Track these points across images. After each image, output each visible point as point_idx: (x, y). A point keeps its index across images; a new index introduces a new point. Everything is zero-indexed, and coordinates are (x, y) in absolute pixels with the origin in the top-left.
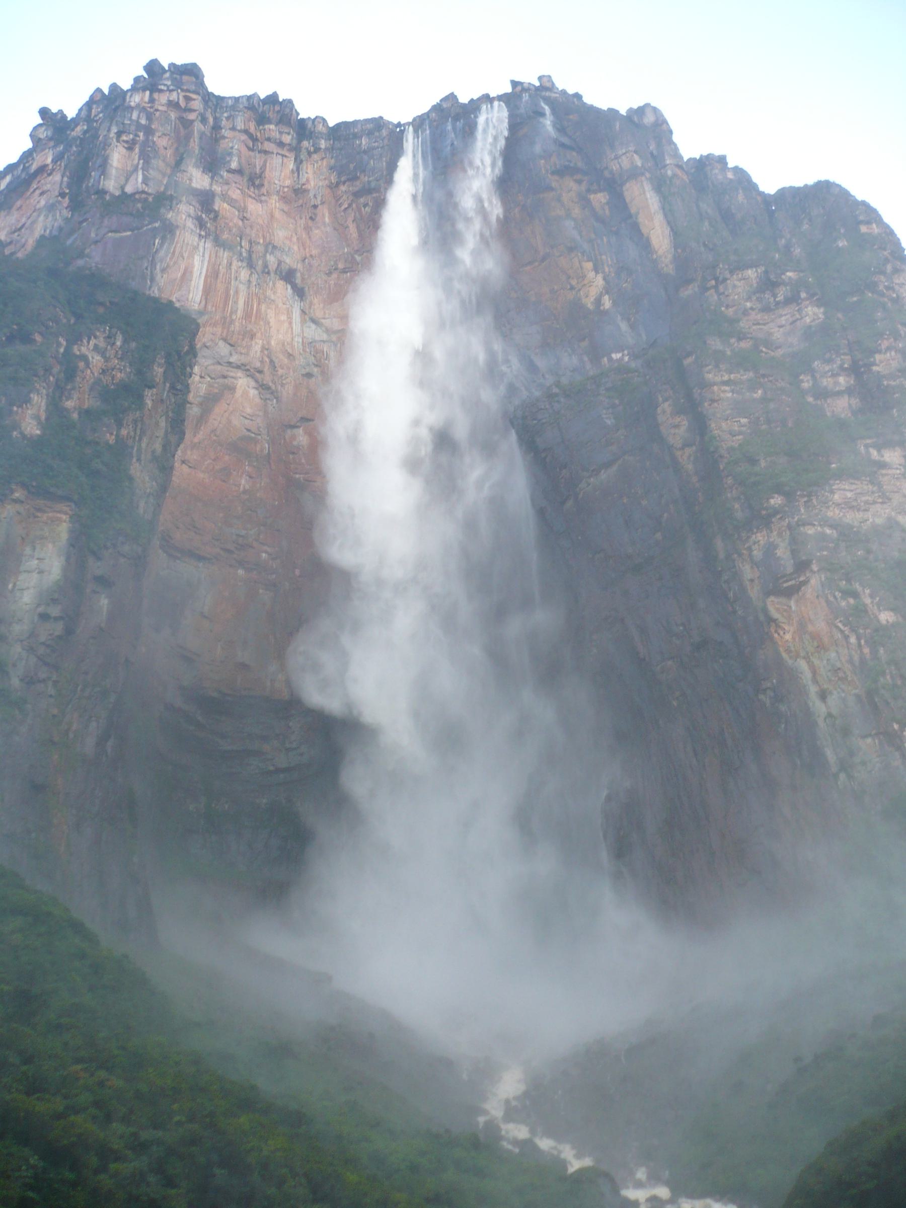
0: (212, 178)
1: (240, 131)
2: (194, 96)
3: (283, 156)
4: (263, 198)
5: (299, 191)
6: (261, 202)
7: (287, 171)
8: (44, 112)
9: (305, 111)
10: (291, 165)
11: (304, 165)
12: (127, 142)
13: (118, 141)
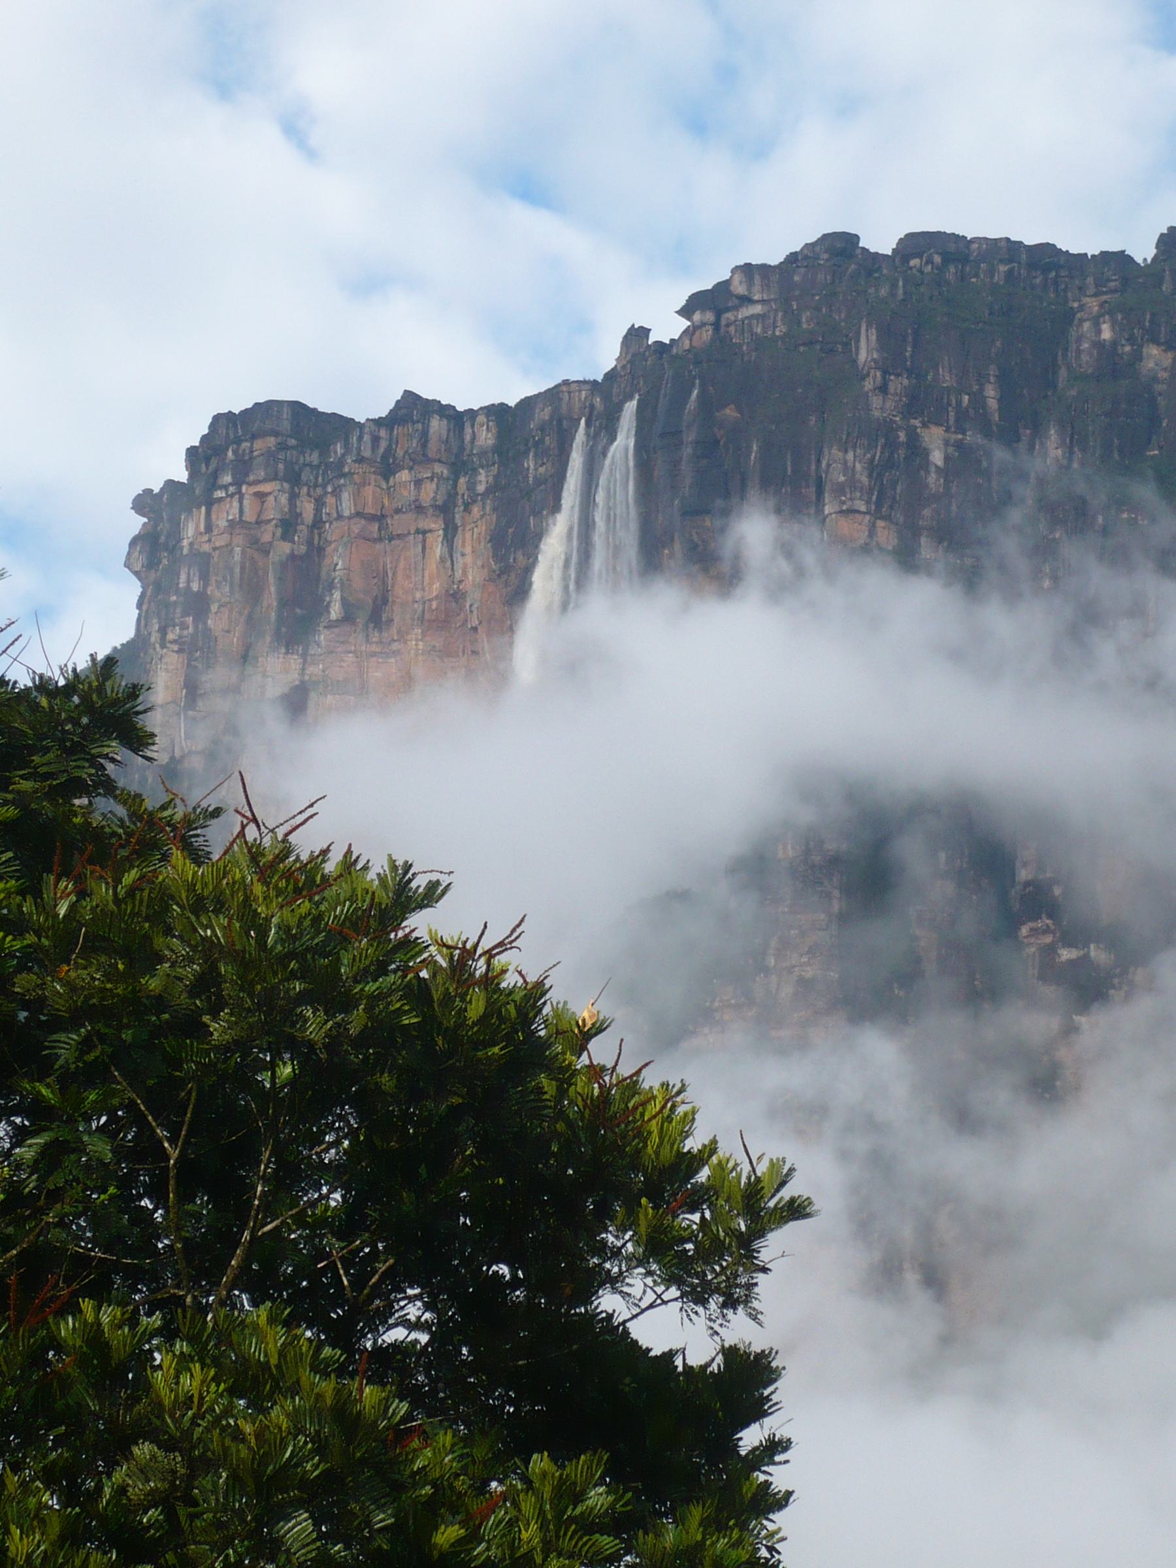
0: (304, 656)
1: (349, 518)
2: (266, 488)
3: (424, 532)
4: (395, 646)
5: (455, 596)
6: (397, 653)
7: (432, 565)
8: (144, 503)
9: (465, 396)
10: (437, 549)
11: (458, 540)
12: (174, 642)
13: (163, 646)
